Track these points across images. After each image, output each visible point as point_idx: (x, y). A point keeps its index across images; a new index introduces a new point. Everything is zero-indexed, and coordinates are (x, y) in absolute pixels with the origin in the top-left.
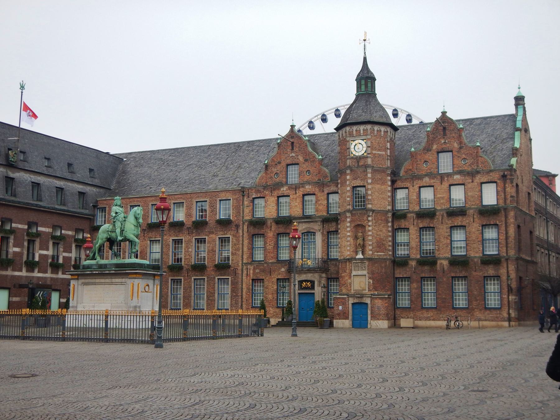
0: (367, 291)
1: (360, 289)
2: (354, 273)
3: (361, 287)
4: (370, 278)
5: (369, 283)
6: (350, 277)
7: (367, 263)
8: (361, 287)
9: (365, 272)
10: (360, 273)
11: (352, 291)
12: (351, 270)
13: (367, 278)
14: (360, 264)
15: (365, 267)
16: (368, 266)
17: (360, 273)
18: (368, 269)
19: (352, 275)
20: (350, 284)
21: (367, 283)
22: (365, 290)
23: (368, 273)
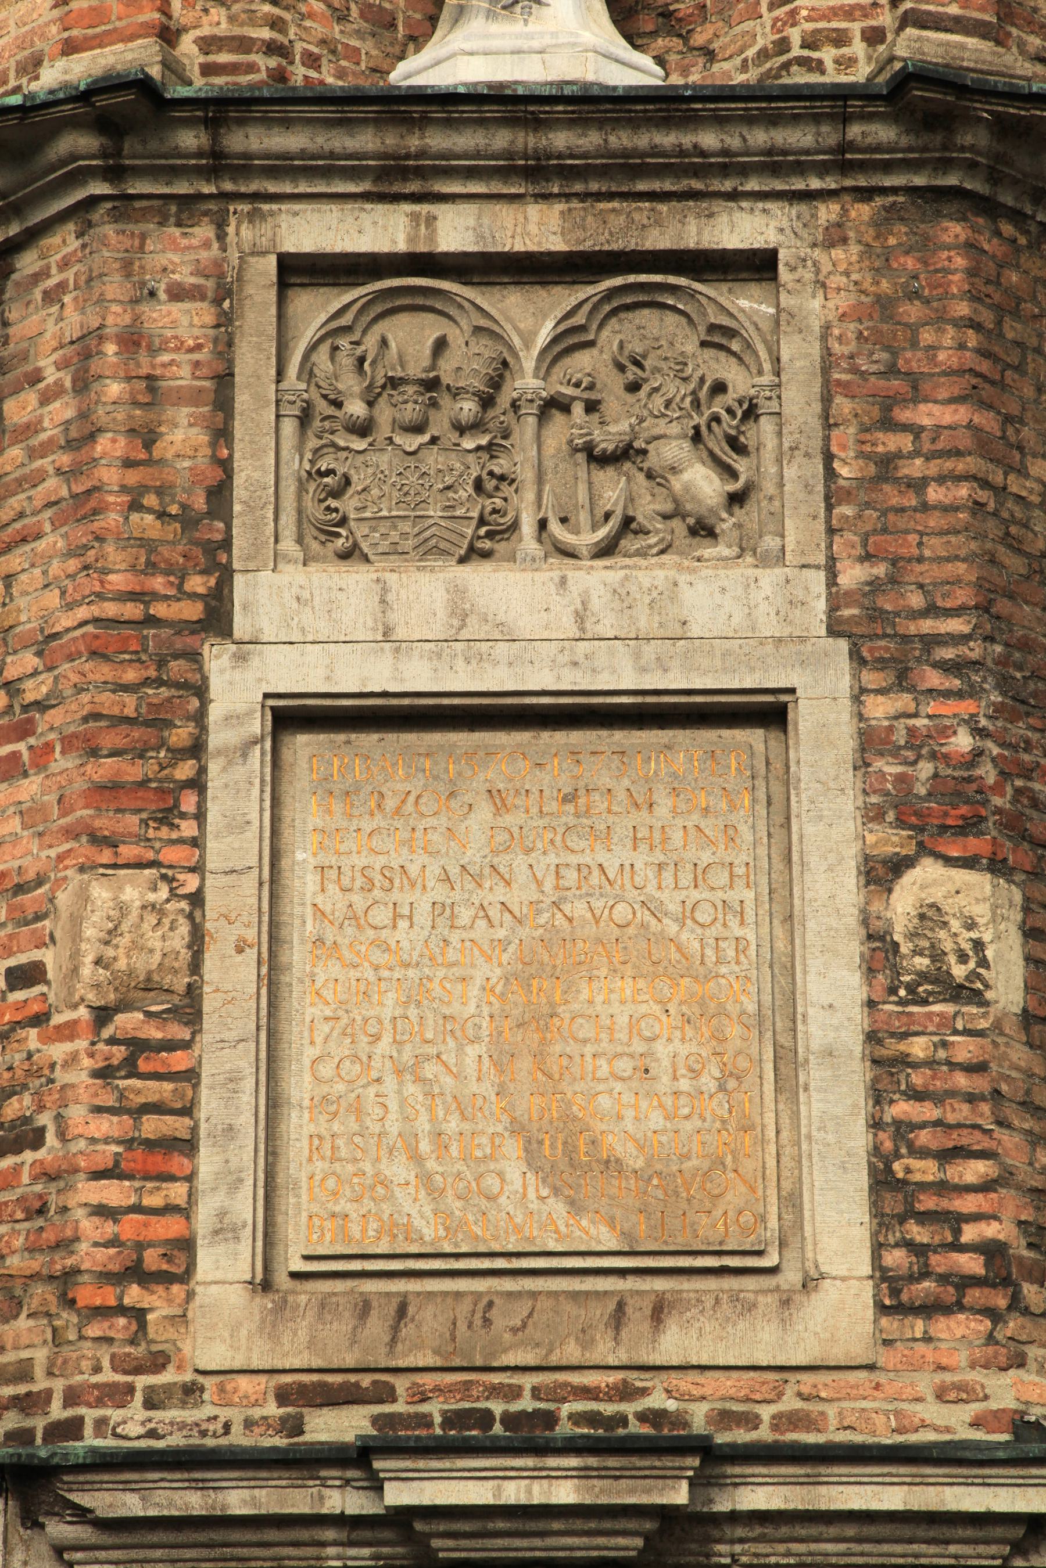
0: (841, 1315)
1: (523, 1211)
2: (307, 622)
3: (569, 1159)
4: (926, 817)
5: (905, 977)
6: (148, 786)
7: (813, 280)
8: (569, 1159)
9: (741, 610)
10: (533, 619)
11: (224, 1328)
12: (203, 540)
13: (833, 827)
14: (531, 318)
15: (728, 433)
16: (875, 384)
17: (533, 619)
18: (868, 501)
19: (236, 690)
20: (149, 1033)
21: (835, 996)
22: (735, 1266)
23: (873, 635)
